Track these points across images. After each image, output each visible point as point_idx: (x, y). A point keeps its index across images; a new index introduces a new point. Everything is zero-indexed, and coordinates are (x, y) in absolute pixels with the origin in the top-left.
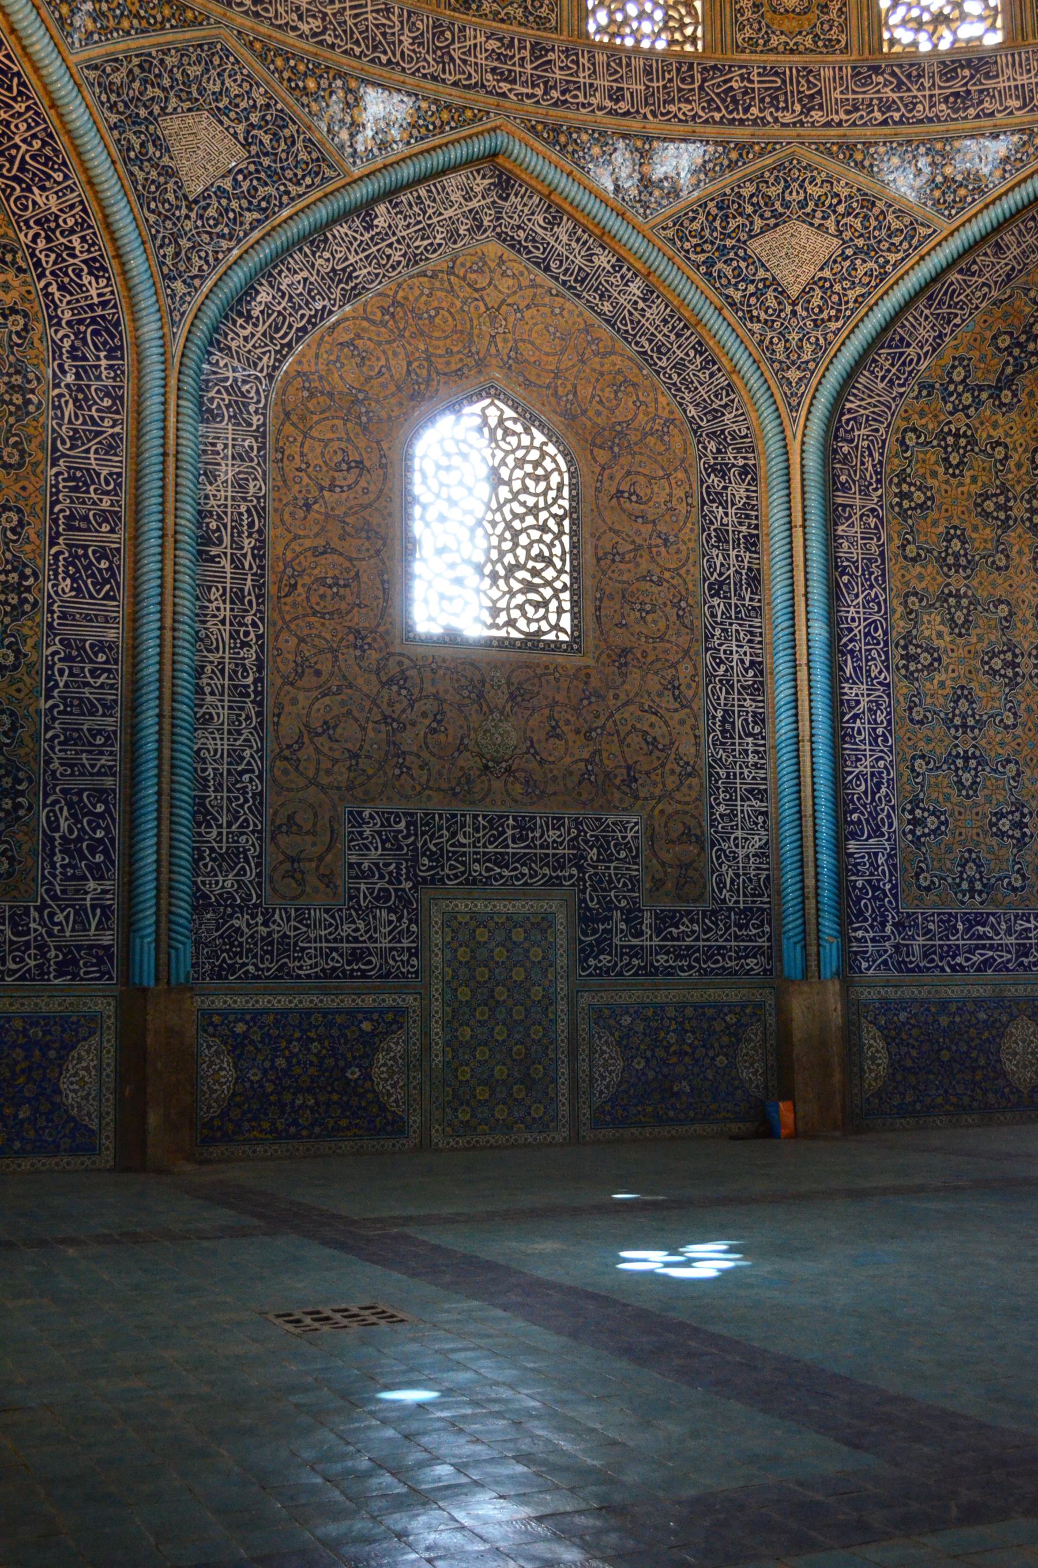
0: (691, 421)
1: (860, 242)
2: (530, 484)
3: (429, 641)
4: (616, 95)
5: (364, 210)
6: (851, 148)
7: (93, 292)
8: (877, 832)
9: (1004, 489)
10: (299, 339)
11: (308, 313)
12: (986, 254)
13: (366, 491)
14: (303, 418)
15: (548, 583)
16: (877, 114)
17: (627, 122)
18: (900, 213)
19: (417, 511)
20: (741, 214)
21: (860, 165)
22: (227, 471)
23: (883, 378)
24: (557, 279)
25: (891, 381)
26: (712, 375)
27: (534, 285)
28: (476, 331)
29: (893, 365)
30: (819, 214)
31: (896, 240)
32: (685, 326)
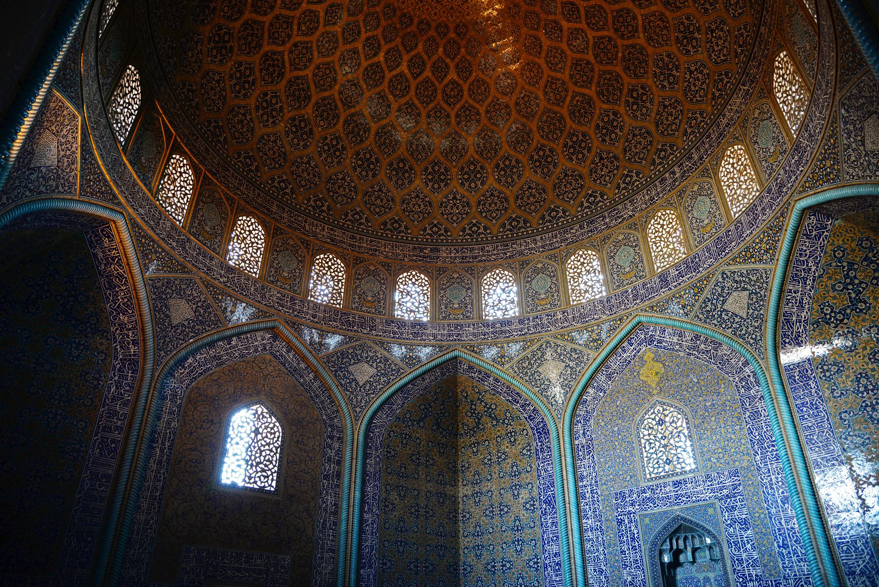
0: (324, 420)
2: (269, 435)
3: (226, 486)
4: (314, 316)
5: (229, 338)
8: (370, 567)
9: (419, 453)
13: (212, 431)
14: (195, 403)
15: (270, 470)
18: (396, 365)
19: (229, 440)
21: (385, 349)
22: (166, 417)
27: (279, 370)
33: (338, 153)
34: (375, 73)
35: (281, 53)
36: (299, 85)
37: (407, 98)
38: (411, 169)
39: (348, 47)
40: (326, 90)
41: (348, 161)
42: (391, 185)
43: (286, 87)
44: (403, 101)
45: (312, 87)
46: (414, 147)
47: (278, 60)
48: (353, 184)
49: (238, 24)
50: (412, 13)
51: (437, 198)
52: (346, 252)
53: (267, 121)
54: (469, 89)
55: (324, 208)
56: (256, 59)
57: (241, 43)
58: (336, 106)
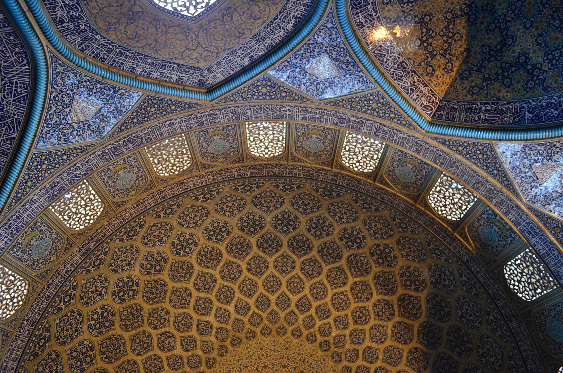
0: (97, 33)
1: (61, 127)
6: (82, 151)
7: (361, 17)
10: (277, 16)
11: (274, 25)
12: (8, 149)
16: (79, 165)
17: (165, 120)
20: (111, 112)
23: (17, 83)
24: (174, 63)
25: (12, 84)
26: (93, 52)
27: (183, 59)
28: (205, 37)
29: (16, 90)
30: (82, 126)
31: (48, 135)
32: (112, 65)
33: (212, 233)
34: (226, 297)
35: (299, 257)
36: (273, 248)
37: (192, 305)
38: (149, 273)
39: (257, 294)
40: (250, 260)
41: (200, 235)
42: (154, 250)
43: (281, 242)
44: (193, 301)
45: (262, 254)
46: (159, 287)
47: (299, 252)
48: (186, 226)
49: (346, 255)
50: (237, 349)
51: (113, 278)
52: (165, 185)
53: (283, 216)
54: (160, 358)
55: (202, 196)
56: (316, 244)
57: (336, 246)
58: (235, 257)
